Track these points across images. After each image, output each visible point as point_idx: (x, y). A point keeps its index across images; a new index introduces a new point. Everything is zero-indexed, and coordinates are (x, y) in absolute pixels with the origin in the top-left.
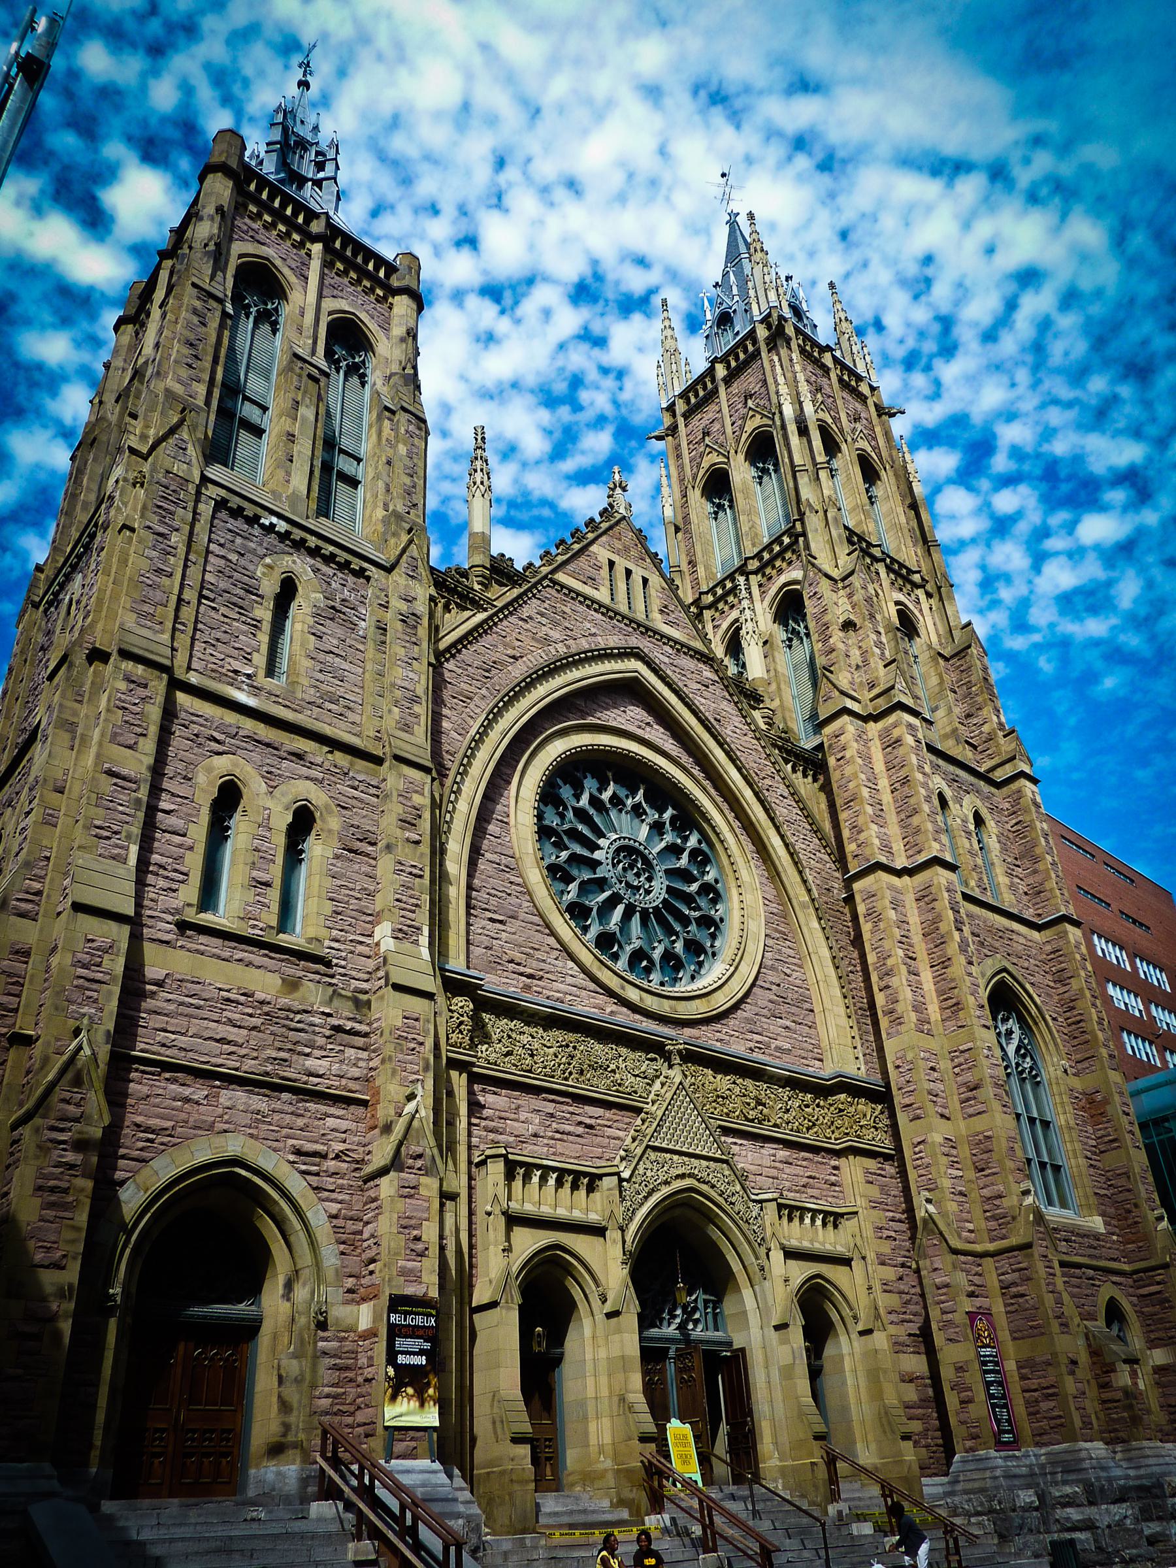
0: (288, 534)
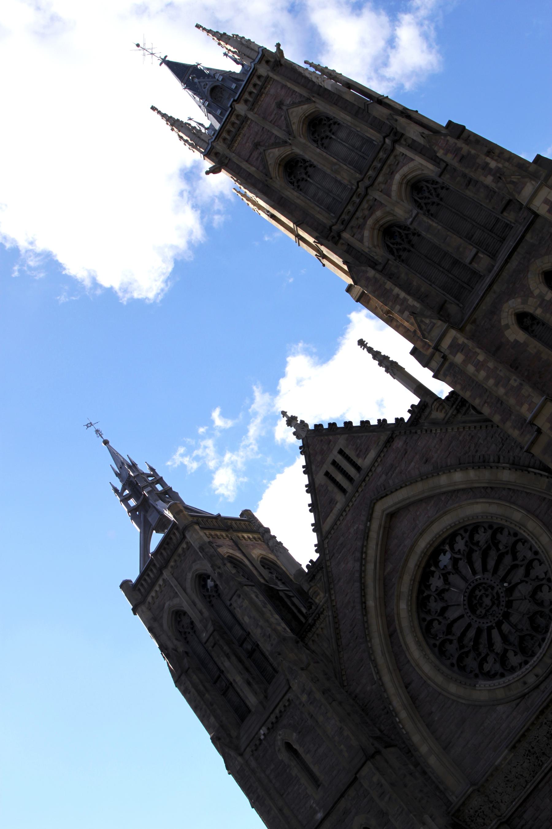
0: (268, 729)
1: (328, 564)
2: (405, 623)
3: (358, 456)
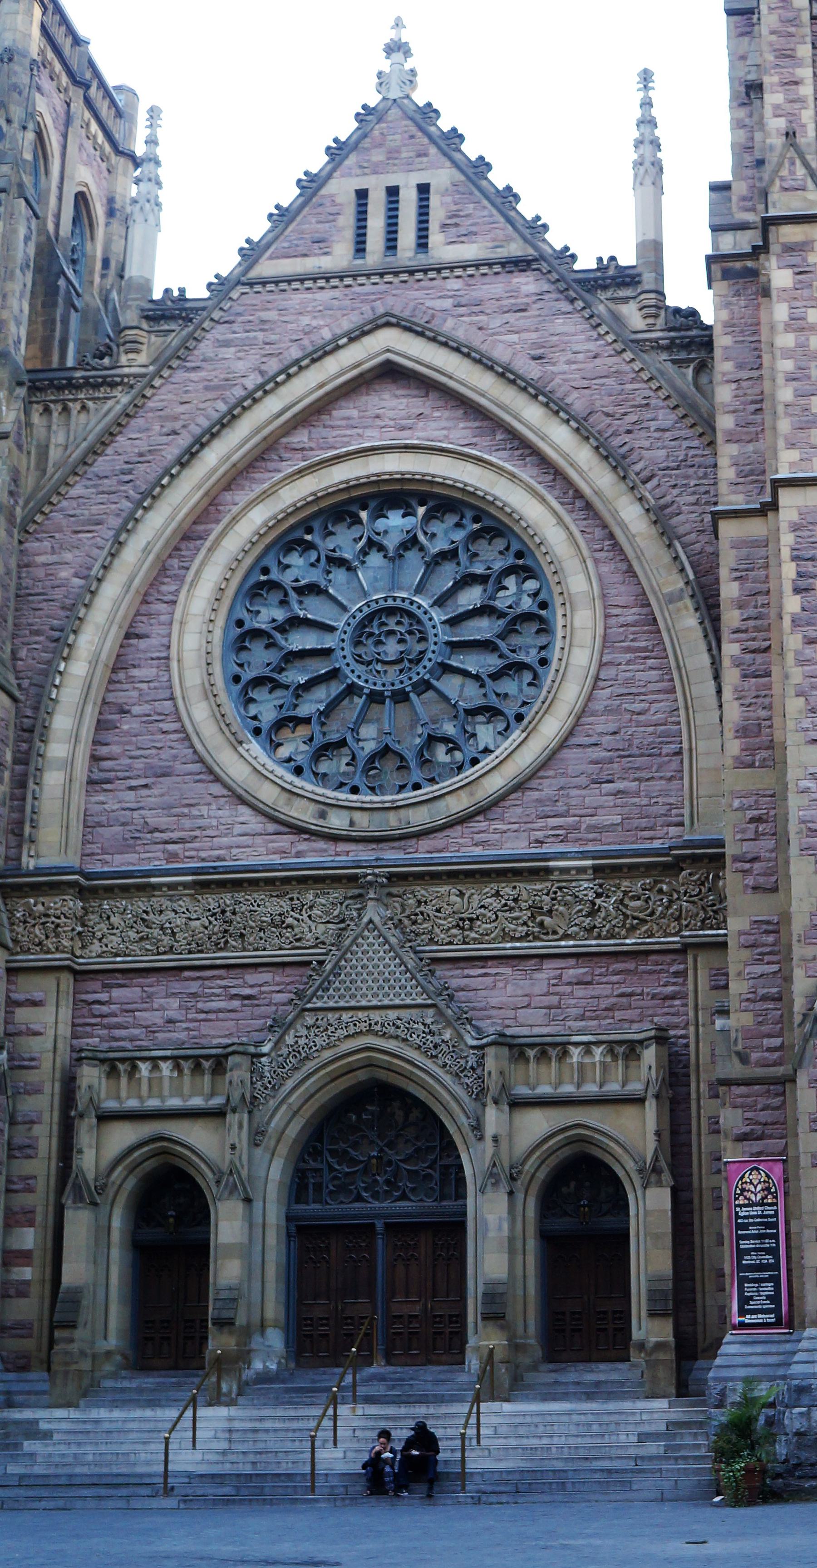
1: (206, 325)
3: (444, 226)
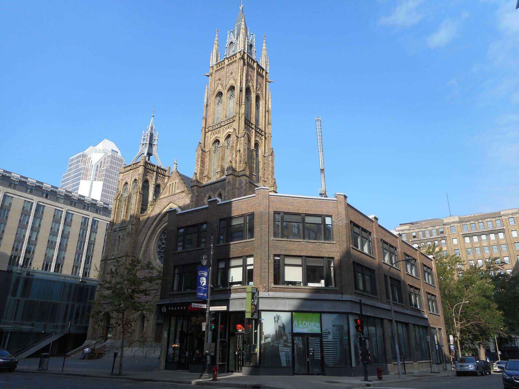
2: (157, 234)
